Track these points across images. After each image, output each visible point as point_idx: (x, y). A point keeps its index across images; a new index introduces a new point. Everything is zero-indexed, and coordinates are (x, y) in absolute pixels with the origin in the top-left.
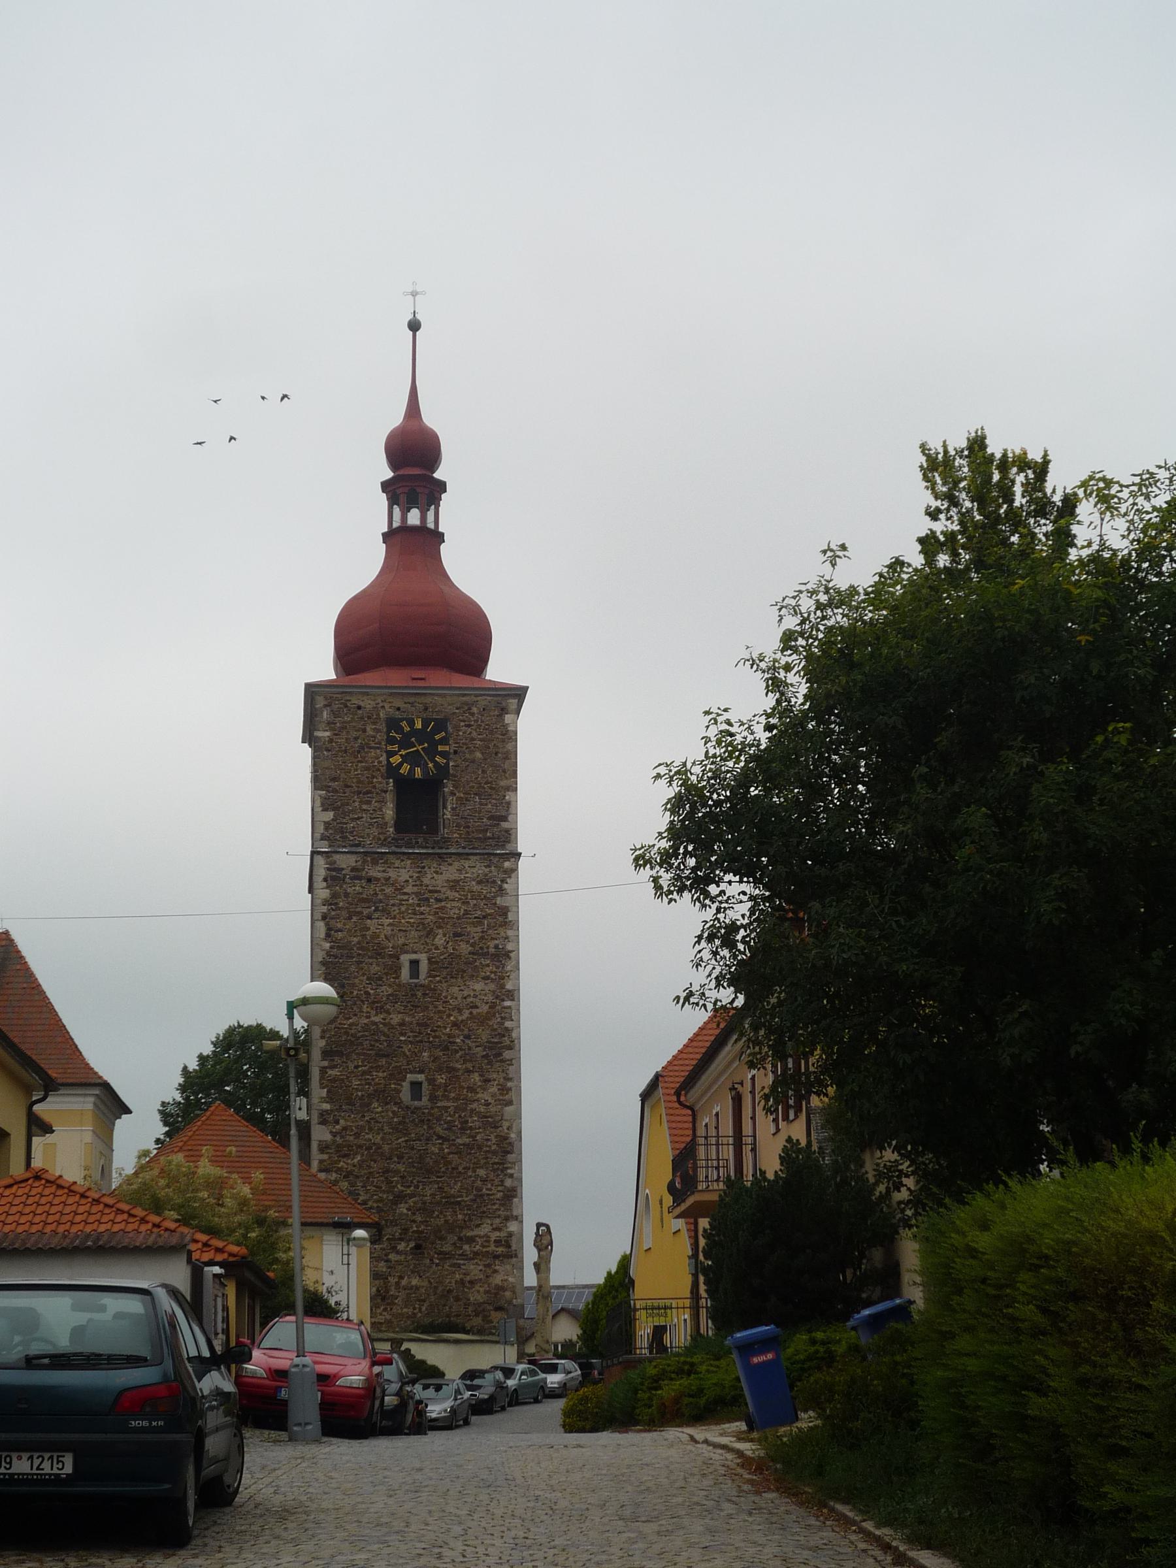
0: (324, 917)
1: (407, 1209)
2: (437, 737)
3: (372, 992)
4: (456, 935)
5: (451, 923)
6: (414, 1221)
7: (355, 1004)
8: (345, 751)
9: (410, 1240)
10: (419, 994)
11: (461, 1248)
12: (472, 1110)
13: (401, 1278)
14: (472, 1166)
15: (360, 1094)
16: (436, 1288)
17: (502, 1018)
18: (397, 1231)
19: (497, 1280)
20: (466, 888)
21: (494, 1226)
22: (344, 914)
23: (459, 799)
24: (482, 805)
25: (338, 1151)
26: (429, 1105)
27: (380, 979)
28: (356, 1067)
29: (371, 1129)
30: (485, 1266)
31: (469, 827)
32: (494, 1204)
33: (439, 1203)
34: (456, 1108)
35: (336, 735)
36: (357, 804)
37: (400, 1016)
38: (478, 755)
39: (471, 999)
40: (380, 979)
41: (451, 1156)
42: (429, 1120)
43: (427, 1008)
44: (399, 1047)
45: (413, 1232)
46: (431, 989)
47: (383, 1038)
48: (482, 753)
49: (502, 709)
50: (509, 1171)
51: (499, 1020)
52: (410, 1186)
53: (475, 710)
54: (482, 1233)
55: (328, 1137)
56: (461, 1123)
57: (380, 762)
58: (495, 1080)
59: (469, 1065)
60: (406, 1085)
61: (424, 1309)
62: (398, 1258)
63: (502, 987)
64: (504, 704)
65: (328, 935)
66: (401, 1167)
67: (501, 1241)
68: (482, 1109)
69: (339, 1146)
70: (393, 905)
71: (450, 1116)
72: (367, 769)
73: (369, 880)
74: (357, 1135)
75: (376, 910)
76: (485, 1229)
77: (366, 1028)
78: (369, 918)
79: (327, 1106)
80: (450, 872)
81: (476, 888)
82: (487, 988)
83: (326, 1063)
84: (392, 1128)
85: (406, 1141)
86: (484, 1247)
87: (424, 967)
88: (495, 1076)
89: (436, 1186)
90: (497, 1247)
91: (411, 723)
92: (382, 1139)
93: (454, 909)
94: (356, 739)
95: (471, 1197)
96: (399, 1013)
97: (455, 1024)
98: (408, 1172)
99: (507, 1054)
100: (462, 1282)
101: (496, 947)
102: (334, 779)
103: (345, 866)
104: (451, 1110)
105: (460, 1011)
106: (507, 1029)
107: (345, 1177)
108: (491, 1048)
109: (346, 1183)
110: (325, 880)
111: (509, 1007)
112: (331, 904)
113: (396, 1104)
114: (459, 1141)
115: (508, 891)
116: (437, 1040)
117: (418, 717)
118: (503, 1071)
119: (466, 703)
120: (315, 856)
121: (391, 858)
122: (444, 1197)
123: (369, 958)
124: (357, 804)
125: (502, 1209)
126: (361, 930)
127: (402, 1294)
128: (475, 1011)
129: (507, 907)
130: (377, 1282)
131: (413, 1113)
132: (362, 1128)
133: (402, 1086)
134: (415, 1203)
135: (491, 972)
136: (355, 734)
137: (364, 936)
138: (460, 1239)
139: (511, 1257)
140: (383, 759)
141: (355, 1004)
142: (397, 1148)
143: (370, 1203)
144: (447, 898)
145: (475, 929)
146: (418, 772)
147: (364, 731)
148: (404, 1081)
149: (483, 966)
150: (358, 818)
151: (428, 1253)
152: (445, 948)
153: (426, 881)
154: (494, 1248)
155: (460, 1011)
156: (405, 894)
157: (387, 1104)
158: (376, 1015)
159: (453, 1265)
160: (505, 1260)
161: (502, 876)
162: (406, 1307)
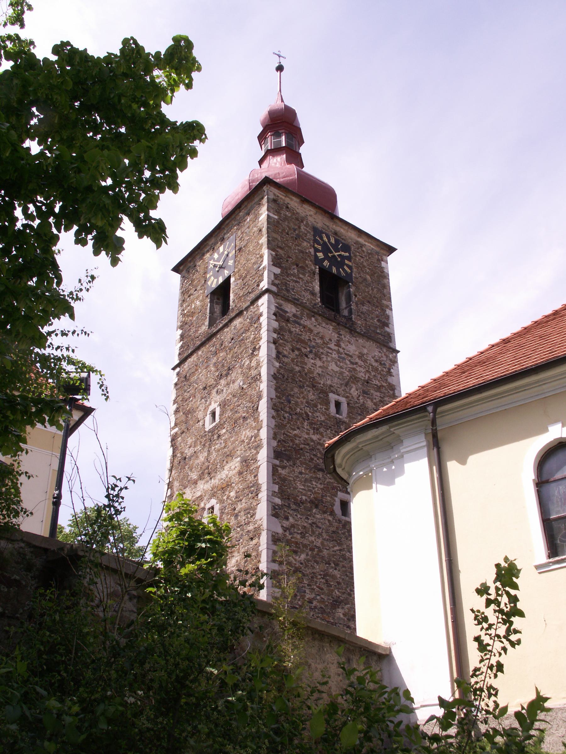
1: (343, 614)
74: (303, 535)
75: (311, 352)
77: (306, 443)
85: (340, 550)
87: (344, 408)
92: (322, 543)
141: (298, 419)
142: (334, 555)
143: (315, 603)
158: (314, 434)
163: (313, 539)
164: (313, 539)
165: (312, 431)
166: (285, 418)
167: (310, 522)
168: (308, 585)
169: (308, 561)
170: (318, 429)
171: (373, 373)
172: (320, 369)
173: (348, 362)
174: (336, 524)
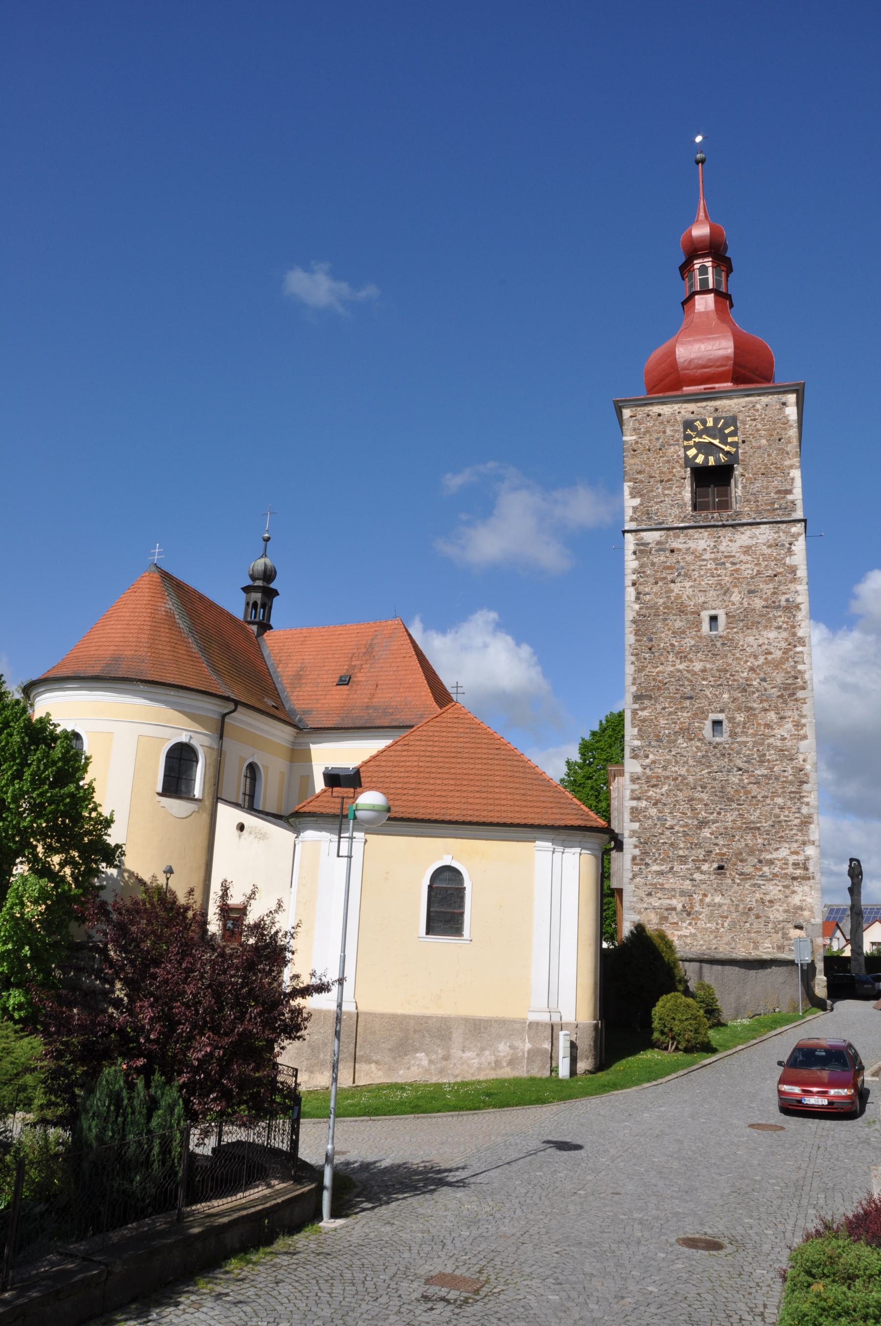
0: (634, 584)
2: (727, 431)
4: (750, 592)
5: (745, 582)
6: (716, 844)
7: (662, 655)
8: (649, 450)
9: (713, 861)
10: (719, 644)
11: (761, 870)
12: (769, 745)
13: (705, 895)
14: (770, 795)
15: (667, 732)
17: (796, 662)
18: (701, 853)
19: (796, 900)
20: (758, 552)
21: (792, 850)
22: (652, 580)
23: (747, 479)
26: (730, 740)
27: (684, 632)
28: (664, 709)
29: (677, 762)
30: (784, 886)
31: (757, 501)
32: (792, 830)
33: (740, 828)
34: (754, 742)
36: (660, 490)
37: (701, 663)
38: (764, 442)
39: (766, 647)
40: (684, 632)
41: (751, 786)
42: (729, 754)
43: (726, 656)
44: (701, 690)
45: (717, 854)
47: (687, 683)
48: (768, 441)
50: (806, 800)
51: (792, 663)
52: (712, 813)
53: (758, 406)
54: (781, 857)
55: (639, 770)
56: (760, 756)
57: (679, 456)
58: (790, 717)
59: (766, 705)
60: (708, 724)
61: (726, 925)
62: (703, 877)
63: (794, 634)
64: (784, 400)
65: (637, 598)
66: (705, 796)
67: (798, 864)
68: (779, 743)
69: (648, 777)
70: (694, 570)
71: (749, 749)
72: (668, 462)
73: (672, 551)
74: (665, 768)
75: (679, 575)
76: (783, 853)
77: (671, 674)
78: (673, 582)
79: (637, 743)
80: (744, 537)
81: (767, 551)
82: (780, 636)
83: (636, 706)
84: (697, 762)
85: (710, 772)
86: (782, 869)
88: (790, 713)
89: (737, 813)
90: (795, 869)
91: (704, 422)
92: (688, 771)
93: (748, 570)
94: (658, 439)
95: (770, 823)
96: (701, 661)
97: (752, 669)
98: (712, 800)
99: (800, 694)
101: (787, 600)
102: (640, 472)
103: (650, 541)
104: (750, 745)
105: (756, 657)
106: (799, 671)
107: (655, 804)
108: (785, 689)
109: (655, 810)
110: (635, 553)
111: (802, 652)
112: (639, 573)
113: (699, 740)
114: (758, 772)
115: (796, 552)
116: (736, 683)
117: (709, 417)
118: (797, 709)
121: (691, 531)
122: (745, 823)
123: (674, 615)
124: (660, 490)
125: (800, 834)
126: (667, 592)
127: (706, 911)
128: (769, 657)
130: (683, 899)
132: (668, 762)
133: (705, 724)
134: (717, 828)
135: (783, 622)
136: (655, 436)
137: (668, 597)
138: (760, 861)
139: (809, 878)
140: (681, 453)
141: (662, 655)
142: (700, 780)
143: (677, 828)
144: (741, 561)
145: (768, 586)
146: (712, 461)
147: (664, 432)
148: (705, 719)
149: (775, 617)
150: (661, 502)
151: (730, 874)
152: (741, 604)
153: (722, 548)
154: (792, 871)
155: (756, 657)
156: (704, 560)
157: (692, 740)
158: (681, 663)
159: (754, 885)
160: (803, 882)
162: (710, 921)
163: (677, 769)
164: (677, 769)
165: (678, 661)
166: (645, 659)
167: (673, 753)
168: (670, 813)
169: (670, 791)
171: (764, 564)
172: (691, 590)
173: (728, 565)
174: (704, 748)
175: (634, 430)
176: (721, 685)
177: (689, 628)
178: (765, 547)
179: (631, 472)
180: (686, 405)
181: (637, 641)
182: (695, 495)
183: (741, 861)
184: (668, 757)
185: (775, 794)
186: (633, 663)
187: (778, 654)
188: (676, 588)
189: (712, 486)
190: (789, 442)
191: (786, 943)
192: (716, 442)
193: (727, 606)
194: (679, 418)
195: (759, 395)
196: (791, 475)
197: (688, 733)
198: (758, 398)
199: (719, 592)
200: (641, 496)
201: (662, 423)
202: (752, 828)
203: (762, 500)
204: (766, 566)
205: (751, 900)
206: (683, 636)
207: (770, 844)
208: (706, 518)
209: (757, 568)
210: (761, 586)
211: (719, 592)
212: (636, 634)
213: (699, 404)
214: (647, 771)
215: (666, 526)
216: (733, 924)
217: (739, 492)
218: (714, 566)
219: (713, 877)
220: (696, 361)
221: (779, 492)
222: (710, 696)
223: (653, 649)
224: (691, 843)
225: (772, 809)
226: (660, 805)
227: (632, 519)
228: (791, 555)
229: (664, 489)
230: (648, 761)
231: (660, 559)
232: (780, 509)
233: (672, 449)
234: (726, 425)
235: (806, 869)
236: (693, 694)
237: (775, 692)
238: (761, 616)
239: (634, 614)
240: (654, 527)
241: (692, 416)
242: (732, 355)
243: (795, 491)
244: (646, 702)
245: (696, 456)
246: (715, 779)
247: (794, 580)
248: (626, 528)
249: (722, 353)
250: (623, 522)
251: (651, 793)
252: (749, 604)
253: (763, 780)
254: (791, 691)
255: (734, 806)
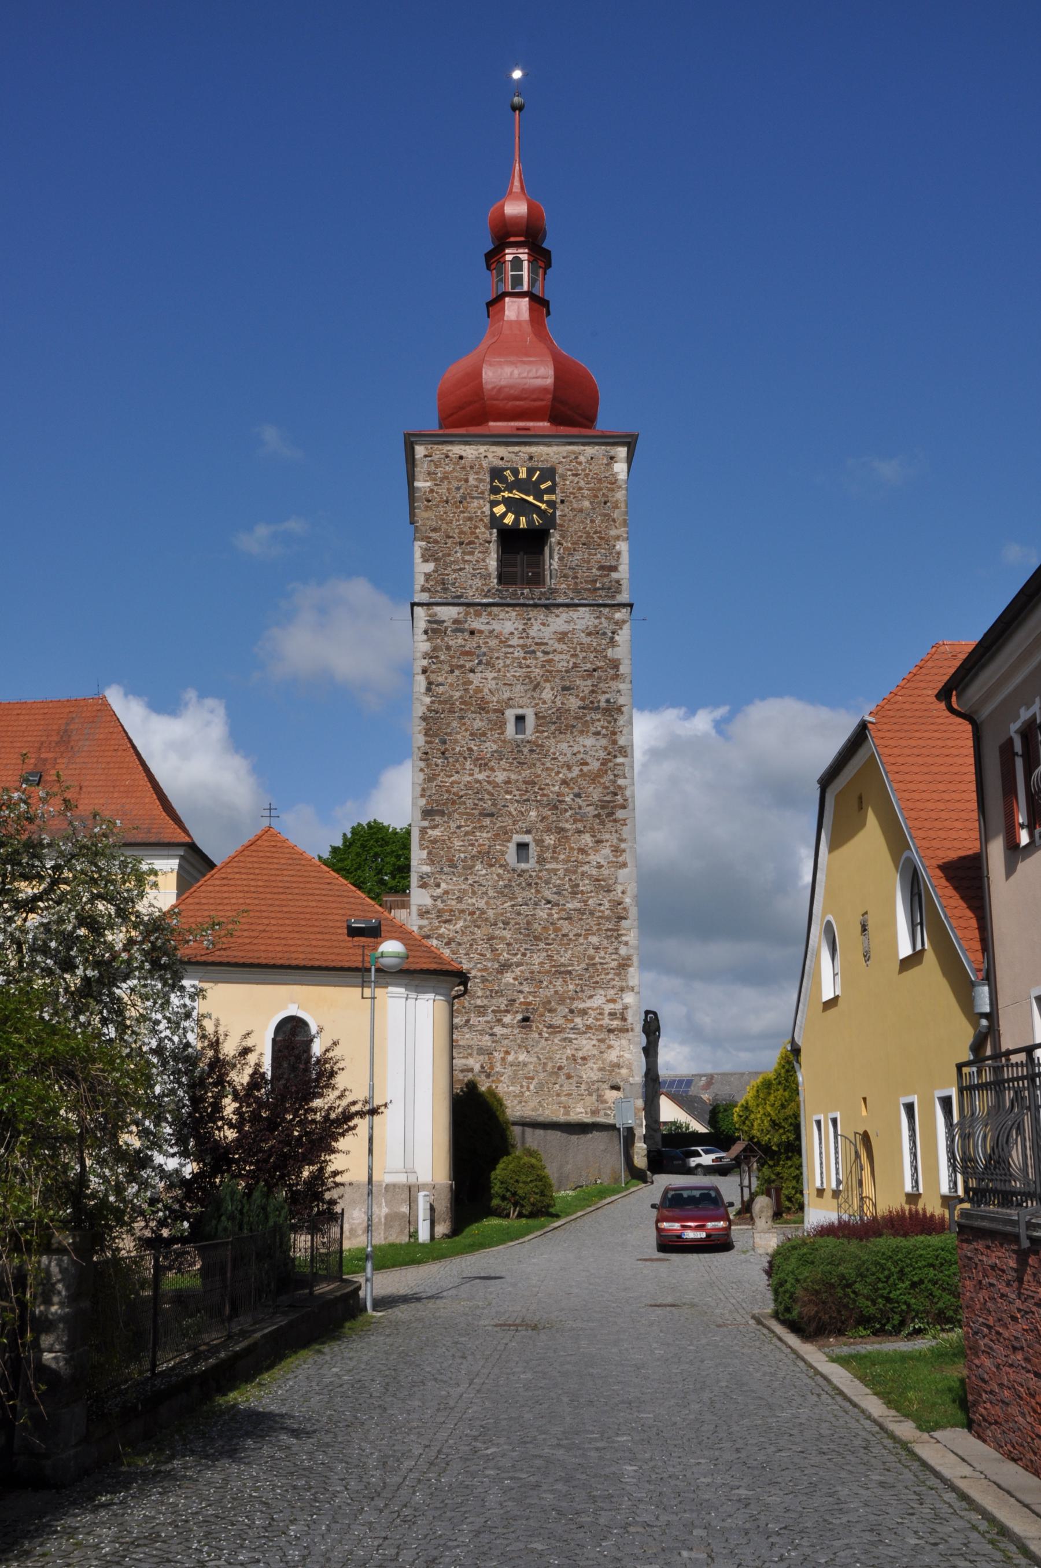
0: (424, 672)
2: (543, 487)
3: (475, 748)
4: (565, 688)
5: (559, 677)
6: (521, 992)
7: (457, 761)
8: (447, 502)
9: (517, 1012)
10: (526, 750)
11: (572, 1021)
13: (507, 1053)
14: (583, 932)
15: (462, 855)
16: (545, 1064)
17: (615, 776)
18: (502, 1002)
19: (612, 1056)
20: (575, 641)
21: (608, 998)
22: (447, 668)
23: (566, 549)
24: (590, 554)
25: (438, 917)
26: (538, 867)
27: (484, 734)
28: (459, 827)
30: (599, 1040)
31: (577, 577)
32: (608, 974)
33: (549, 972)
34: (566, 870)
35: (436, 485)
36: (459, 555)
37: (505, 773)
38: (586, 504)
39: (582, 756)
40: (484, 734)
41: (561, 921)
42: (536, 884)
43: (534, 765)
44: (504, 806)
45: (521, 1003)
46: (538, 746)
47: (487, 797)
48: (591, 503)
49: (612, 458)
51: (612, 777)
52: (516, 954)
53: (582, 459)
54: (595, 1006)
55: (428, 902)
56: (572, 887)
58: (607, 841)
59: (580, 826)
60: (512, 847)
62: (505, 1031)
63: (614, 742)
64: (612, 453)
65: (429, 689)
66: (507, 934)
67: (615, 1014)
68: (594, 872)
69: (439, 911)
70: (498, 658)
71: (560, 878)
72: (470, 519)
73: (472, 633)
74: (460, 900)
75: (480, 663)
76: (598, 1001)
77: (468, 786)
78: (472, 671)
79: (427, 869)
80: (559, 621)
81: (586, 640)
82: (598, 744)
83: (426, 824)
84: (498, 892)
85: (513, 906)
86: (597, 1020)
88: (607, 836)
89: (545, 954)
90: (611, 1020)
91: (515, 472)
92: (487, 903)
93: (562, 661)
94: (458, 489)
95: (583, 966)
96: (504, 770)
97: (564, 782)
99: (620, 814)
100: (574, 1058)
101: (608, 701)
102: (435, 530)
104: (561, 873)
105: (569, 768)
106: (620, 787)
108: (603, 807)
109: (448, 951)
110: (426, 632)
111: (623, 764)
112: (431, 658)
113: (501, 866)
114: (569, 906)
115: (620, 643)
116: (545, 798)
117: (522, 466)
118: (616, 832)
119: (574, 453)
120: (415, 608)
121: (495, 609)
122: (554, 966)
123: (473, 712)
124: (459, 555)
125: (617, 979)
126: (464, 684)
127: (509, 1071)
128: (585, 769)
129: (618, 660)
130: (481, 1057)
131: (519, 875)
133: (508, 847)
134: (522, 972)
135: (603, 727)
136: (455, 484)
137: (466, 690)
138: (572, 1011)
139: (627, 1031)
140: (487, 509)
141: (457, 761)
142: (502, 914)
144: (555, 651)
145: (586, 683)
146: (523, 522)
147: (467, 481)
148: (509, 841)
150: (461, 569)
151: (537, 1027)
152: (554, 702)
154: (609, 1022)
155: (569, 768)
156: (510, 646)
157: (492, 866)
158: (480, 772)
159: (565, 1039)
160: (621, 1035)
161: (613, 627)
162: (513, 1084)
163: (474, 901)
164: (474, 901)
165: (477, 770)
166: (437, 765)
167: (470, 882)
168: (466, 955)
170: (486, 764)
171: (581, 655)
172: (494, 682)
173: (539, 654)
174: (507, 876)
175: (429, 474)
176: (528, 800)
177: (491, 729)
178: (583, 635)
179: (423, 529)
180: (494, 448)
181: (427, 742)
182: (501, 562)
183: (550, 1011)
184: (463, 887)
185: (589, 932)
186: (422, 770)
187: (595, 765)
188: (476, 679)
189: (521, 553)
190: (616, 507)
191: (601, 1106)
192: (531, 499)
193: (537, 704)
194: (485, 464)
195: (584, 444)
196: (618, 547)
197: (487, 857)
198: (582, 448)
199: (528, 687)
200: (436, 560)
201: (463, 468)
202: (563, 972)
203: (582, 577)
204: (584, 658)
205: (562, 1057)
206: (483, 738)
207: (582, 991)
208: (514, 594)
209: (573, 660)
210: (578, 683)
211: (528, 687)
212: (426, 735)
213: (511, 449)
214: (439, 903)
215: (466, 601)
216: (541, 1086)
217: (555, 564)
218: (522, 655)
219: (516, 1031)
220: (507, 390)
221: (602, 568)
222: (514, 813)
223: (447, 755)
224: (491, 991)
225: (586, 950)
226: (453, 945)
227: (424, 590)
228: (613, 646)
229: (464, 553)
230: (439, 891)
231: (457, 641)
232: (602, 589)
233: (475, 503)
234: (542, 479)
235: (624, 1019)
236: (494, 810)
237: (591, 811)
238: (576, 718)
239: (424, 709)
240: (450, 600)
241: (501, 463)
242: (552, 388)
243: (620, 568)
244: (437, 818)
245: (504, 515)
246: (519, 914)
247: (616, 677)
248: (416, 600)
249: (539, 382)
250: (412, 592)
251: (442, 930)
252: (562, 703)
253: (575, 915)
254: (609, 810)
255: (542, 945)
